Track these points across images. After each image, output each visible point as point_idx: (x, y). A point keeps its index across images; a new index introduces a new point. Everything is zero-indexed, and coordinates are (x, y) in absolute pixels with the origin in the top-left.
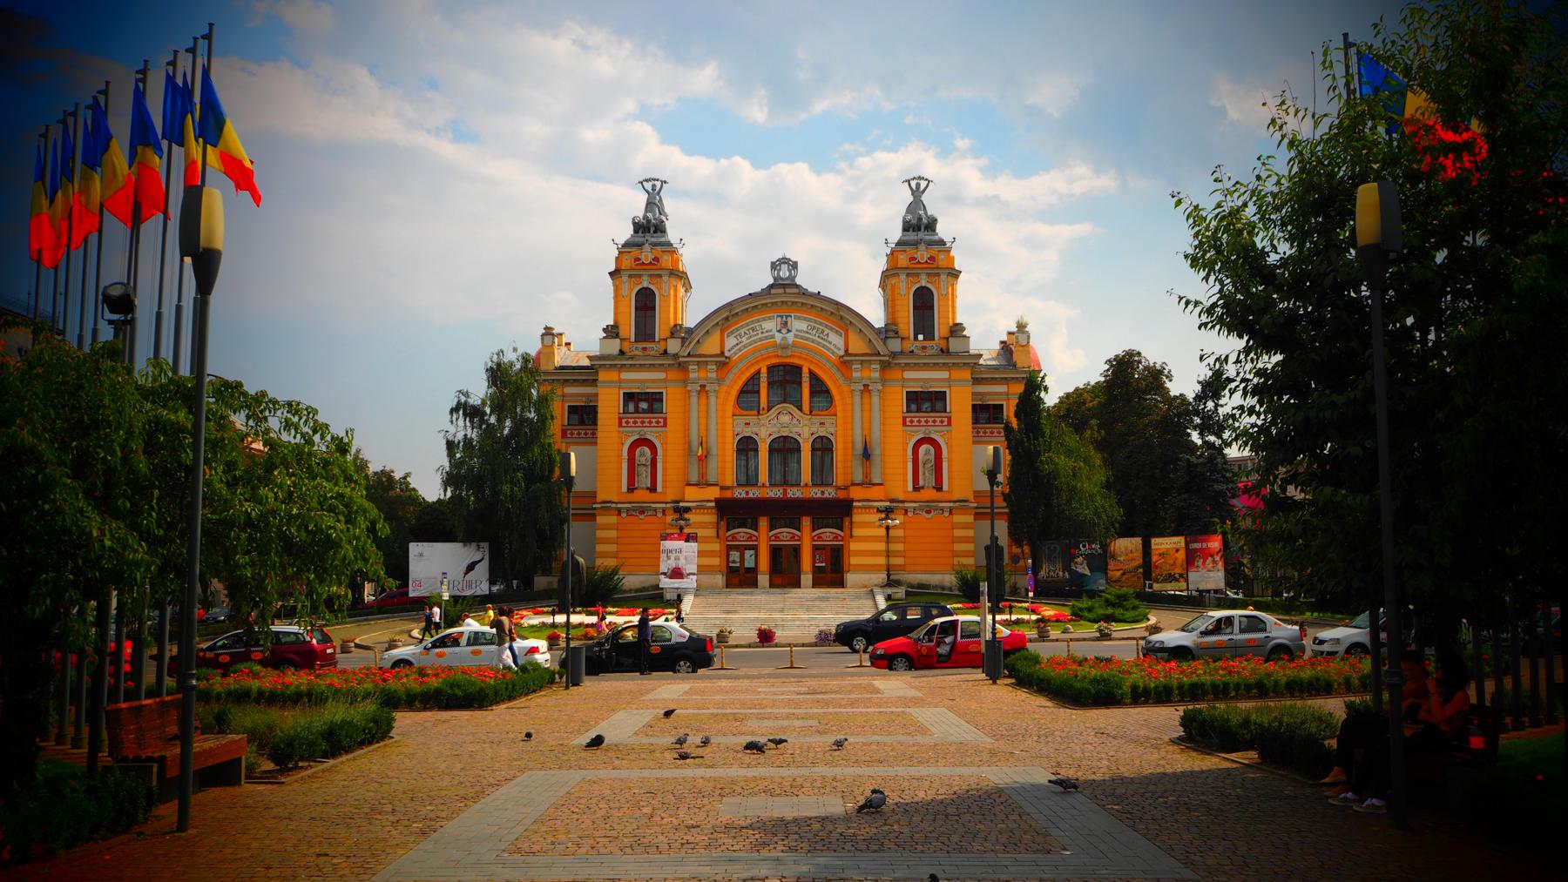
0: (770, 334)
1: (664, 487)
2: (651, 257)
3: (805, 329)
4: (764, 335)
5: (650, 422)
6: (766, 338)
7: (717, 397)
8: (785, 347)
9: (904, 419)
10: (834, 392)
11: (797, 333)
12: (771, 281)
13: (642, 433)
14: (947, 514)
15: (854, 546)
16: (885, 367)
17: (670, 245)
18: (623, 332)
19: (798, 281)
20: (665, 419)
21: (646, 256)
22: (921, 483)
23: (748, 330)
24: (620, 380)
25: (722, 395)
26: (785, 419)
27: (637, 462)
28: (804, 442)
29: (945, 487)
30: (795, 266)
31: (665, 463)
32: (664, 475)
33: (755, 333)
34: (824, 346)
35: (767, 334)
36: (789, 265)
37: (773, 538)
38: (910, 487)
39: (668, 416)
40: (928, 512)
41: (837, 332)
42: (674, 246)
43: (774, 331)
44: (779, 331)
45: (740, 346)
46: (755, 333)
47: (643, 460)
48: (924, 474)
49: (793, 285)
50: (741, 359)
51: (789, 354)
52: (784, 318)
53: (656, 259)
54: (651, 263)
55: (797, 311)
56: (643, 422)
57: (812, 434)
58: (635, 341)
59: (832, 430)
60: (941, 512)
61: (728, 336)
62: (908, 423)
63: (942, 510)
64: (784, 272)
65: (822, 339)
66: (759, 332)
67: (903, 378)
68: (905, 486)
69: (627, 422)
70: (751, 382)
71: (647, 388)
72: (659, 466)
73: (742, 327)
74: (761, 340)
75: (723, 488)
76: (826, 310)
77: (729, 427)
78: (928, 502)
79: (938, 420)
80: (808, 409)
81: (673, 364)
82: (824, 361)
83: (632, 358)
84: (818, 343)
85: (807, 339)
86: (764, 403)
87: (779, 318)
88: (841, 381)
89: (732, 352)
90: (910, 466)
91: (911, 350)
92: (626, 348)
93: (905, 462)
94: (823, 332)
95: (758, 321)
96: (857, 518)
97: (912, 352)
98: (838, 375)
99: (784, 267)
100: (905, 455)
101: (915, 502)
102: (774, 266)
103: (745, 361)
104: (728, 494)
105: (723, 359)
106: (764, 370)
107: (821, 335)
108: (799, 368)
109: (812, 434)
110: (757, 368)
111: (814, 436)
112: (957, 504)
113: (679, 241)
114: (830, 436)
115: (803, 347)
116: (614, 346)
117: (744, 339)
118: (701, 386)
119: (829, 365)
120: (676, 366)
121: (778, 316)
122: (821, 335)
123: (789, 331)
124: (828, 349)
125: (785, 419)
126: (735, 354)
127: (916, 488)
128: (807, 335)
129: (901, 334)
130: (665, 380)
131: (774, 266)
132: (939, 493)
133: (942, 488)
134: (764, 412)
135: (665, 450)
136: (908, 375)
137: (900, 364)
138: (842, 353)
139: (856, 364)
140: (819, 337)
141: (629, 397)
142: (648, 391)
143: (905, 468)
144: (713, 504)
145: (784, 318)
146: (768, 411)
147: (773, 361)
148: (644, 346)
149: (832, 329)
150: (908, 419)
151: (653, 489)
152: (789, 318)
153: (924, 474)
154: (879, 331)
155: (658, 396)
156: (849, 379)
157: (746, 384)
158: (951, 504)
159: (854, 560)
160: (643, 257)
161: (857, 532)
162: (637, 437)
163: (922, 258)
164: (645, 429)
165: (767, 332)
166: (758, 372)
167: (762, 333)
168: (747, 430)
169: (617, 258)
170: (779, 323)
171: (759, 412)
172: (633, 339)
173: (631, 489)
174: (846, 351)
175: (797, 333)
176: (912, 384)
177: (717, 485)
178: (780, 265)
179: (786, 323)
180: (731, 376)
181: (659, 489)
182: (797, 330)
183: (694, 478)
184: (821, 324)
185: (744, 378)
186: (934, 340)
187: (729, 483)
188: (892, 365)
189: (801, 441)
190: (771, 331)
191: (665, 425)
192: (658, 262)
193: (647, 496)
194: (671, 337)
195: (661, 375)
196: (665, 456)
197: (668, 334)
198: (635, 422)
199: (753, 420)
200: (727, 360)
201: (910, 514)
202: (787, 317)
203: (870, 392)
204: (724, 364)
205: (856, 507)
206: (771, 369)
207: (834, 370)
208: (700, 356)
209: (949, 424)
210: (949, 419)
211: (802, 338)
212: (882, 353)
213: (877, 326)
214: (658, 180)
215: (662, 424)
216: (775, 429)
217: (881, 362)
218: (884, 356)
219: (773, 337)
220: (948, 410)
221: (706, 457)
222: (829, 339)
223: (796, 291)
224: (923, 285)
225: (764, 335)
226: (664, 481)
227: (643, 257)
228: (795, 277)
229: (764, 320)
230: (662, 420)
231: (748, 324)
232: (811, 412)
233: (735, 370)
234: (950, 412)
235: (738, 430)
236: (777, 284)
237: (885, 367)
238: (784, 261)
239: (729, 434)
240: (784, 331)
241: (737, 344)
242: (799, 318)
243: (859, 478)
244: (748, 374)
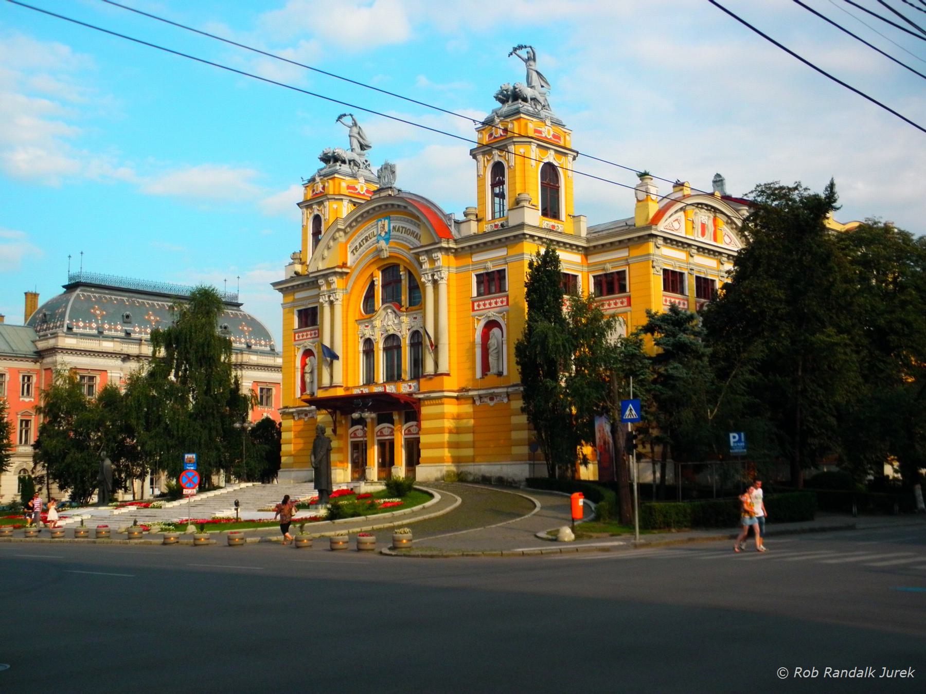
14: (505, 400)
15: (424, 439)
37: (379, 434)
40: (492, 399)
75: (347, 389)
77: (350, 332)
96: (425, 410)
101: (483, 389)
104: (348, 393)
112: (510, 390)
159: (424, 453)
161: (425, 424)
177: (342, 386)
179: (384, 225)
180: (350, 284)
201: (478, 403)
204: (347, 273)
214: (345, 115)
224: (496, 160)
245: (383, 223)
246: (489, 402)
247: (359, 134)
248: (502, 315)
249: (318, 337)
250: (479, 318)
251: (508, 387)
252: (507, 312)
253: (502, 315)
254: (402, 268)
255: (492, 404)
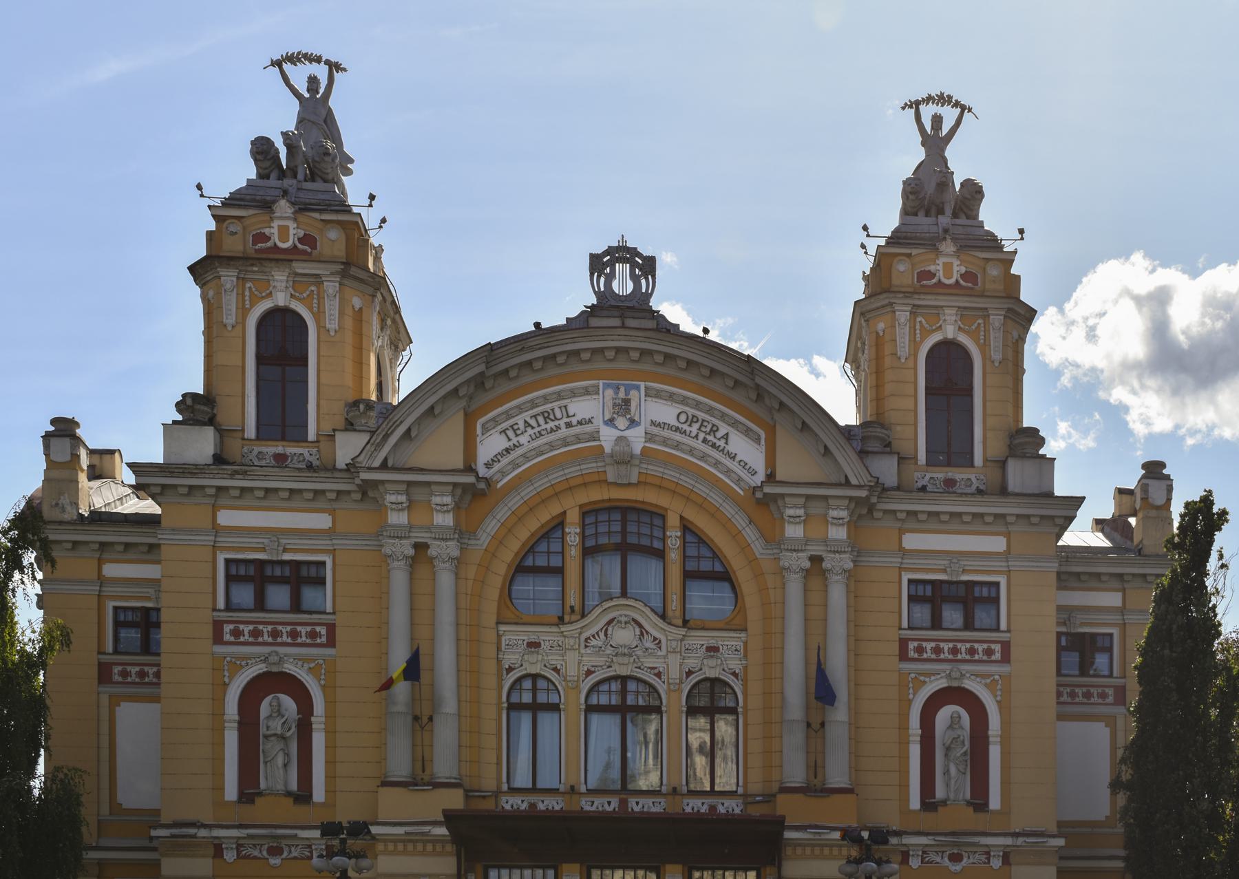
0: (588, 428)
1: (330, 790)
2: (294, 232)
3: (677, 424)
4: (572, 431)
5: (294, 634)
6: (578, 438)
7: (457, 576)
8: (623, 459)
9: (903, 643)
10: (743, 576)
11: (656, 431)
12: (593, 300)
13: (274, 659)
14: (996, 863)
16: (860, 516)
17: (347, 209)
18: (227, 417)
19: (655, 304)
20: (331, 628)
21: (284, 231)
22: (940, 793)
23: (535, 416)
24: (216, 529)
25: (471, 572)
26: (624, 636)
27: (263, 730)
28: (669, 691)
29: (995, 803)
30: (648, 266)
31: (330, 732)
32: (330, 762)
33: (551, 424)
34: (717, 464)
35: (578, 430)
36: (634, 265)
38: (915, 803)
39: (339, 620)
40: (956, 858)
41: (747, 432)
42: (355, 210)
43: (598, 422)
44: (610, 422)
45: (514, 455)
46: (551, 424)
47: (276, 726)
48: (946, 772)
49: (645, 311)
50: (513, 486)
51: (634, 480)
52: (622, 389)
53: (307, 239)
54: (295, 246)
55: (647, 377)
56: (275, 634)
57: (689, 673)
58: (258, 438)
59: (735, 664)
60: (983, 857)
61: (485, 429)
62: (912, 654)
63: (988, 853)
64: (623, 284)
65: (714, 445)
66: (562, 423)
67: (901, 548)
68: (905, 798)
69: (237, 633)
70: (543, 547)
71: (285, 550)
72: (318, 741)
73: (520, 409)
74: (565, 442)
76: (723, 374)
78: (953, 834)
79: (980, 647)
80: (678, 613)
81: (349, 492)
82: (715, 498)
83: (245, 473)
84: (704, 457)
85: (678, 446)
86: (573, 599)
87: (610, 393)
88: (758, 547)
89: (497, 467)
90: (915, 751)
91: (920, 484)
92: (235, 448)
93: (904, 743)
94: (715, 429)
95: (559, 396)
97: (923, 489)
98: (750, 534)
99: (622, 269)
100: (904, 727)
101: (927, 834)
102: (598, 264)
103: (527, 492)
105: (470, 479)
106: (573, 516)
107: (710, 438)
108: (657, 516)
109: (689, 673)
110: (555, 509)
111: (694, 679)
112: (1020, 841)
113: (367, 202)
114: (730, 679)
115: (668, 461)
116: (202, 445)
117: (523, 439)
118: (417, 546)
119: (729, 510)
120: (358, 496)
121: (607, 386)
122: (710, 438)
123: (633, 423)
124: (728, 472)
125: (624, 636)
126: (503, 473)
127: (929, 803)
128: (678, 437)
129: (895, 444)
130: (329, 533)
131: (598, 264)
132: (981, 816)
133: (986, 804)
134: (574, 618)
135: (330, 703)
136: (912, 541)
137: (894, 512)
138: (760, 477)
139: (795, 507)
140: (705, 441)
141: (237, 573)
142: (287, 557)
143: (904, 758)
144: (442, 831)
145: (622, 389)
146: (583, 616)
147: (596, 495)
148: (280, 450)
149: (734, 424)
150: (912, 645)
151: (303, 796)
152: (633, 394)
153: (946, 772)
154: (847, 431)
155: (313, 572)
156: (774, 540)
157: (531, 550)
158: (1009, 841)
160: (273, 231)
162: (260, 668)
163: (948, 274)
164: (282, 650)
165: (580, 423)
166: (559, 524)
167: (569, 425)
168: (533, 658)
169: (210, 235)
170: (609, 404)
171: (561, 619)
172: (251, 432)
173: (249, 791)
174: (771, 477)
175: (656, 431)
176: (922, 563)
178: (611, 264)
179: (627, 402)
180: (491, 526)
181: (319, 794)
182: (653, 423)
183: (400, 766)
184: (710, 411)
185: (524, 533)
186: (972, 465)
187: (489, 784)
188: (877, 515)
189: (662, 688)
190: (590, 421)
191: (331, 643)
192: (314, 247)
193: (288, 810)
194: (346, 430)
195: (321, 521)
196: (330, 716)
197: (340, 422)
198: (256, 633)
199: (547, 635)
200: (482, 485)
202: (628, 389)
203: (824, 573)
205: (796, 843)
206: (588, 512)
207: (740, 521)
208: (421, 470)
209: (1006, 658)
210: (1006, 646)
211: (665, 442)
212: (854, 481)
213: (842, 423)
215: (324, 639)
216: (600, 661)
217: (858, 501)
218: (859, 487)
219: (595, 436)
220: (1003, 626)
221: (431, 719)
222: (731, 448)
223: (651, 324)
225: (572, 431)
226: (330, 777)
227: (275, 231)
228: (648, 295)
229: (574, 394)
230: (322, 630)
231: (533, 404)
232: (685, 623)
233: (503, 513)
234: (1009, 631)
235: (510, 659)
236: (606, 305)
237: (860, 516)
238: (622, 253)
239: (489, 667)
240: (622, 422)
241: (508, 450)
242: (658, 395)
243: (796, 774)
244: (534, 524)
245: (622, 395)
246: (946, 862)
247: (325, 121)
248: (988, 681)
249: (331, 643)
250: (922, 678)
251: (1016, 835)
252: (1006, 678)
253: (988, 681)
254: (673, 520)
255: (957, 868)
